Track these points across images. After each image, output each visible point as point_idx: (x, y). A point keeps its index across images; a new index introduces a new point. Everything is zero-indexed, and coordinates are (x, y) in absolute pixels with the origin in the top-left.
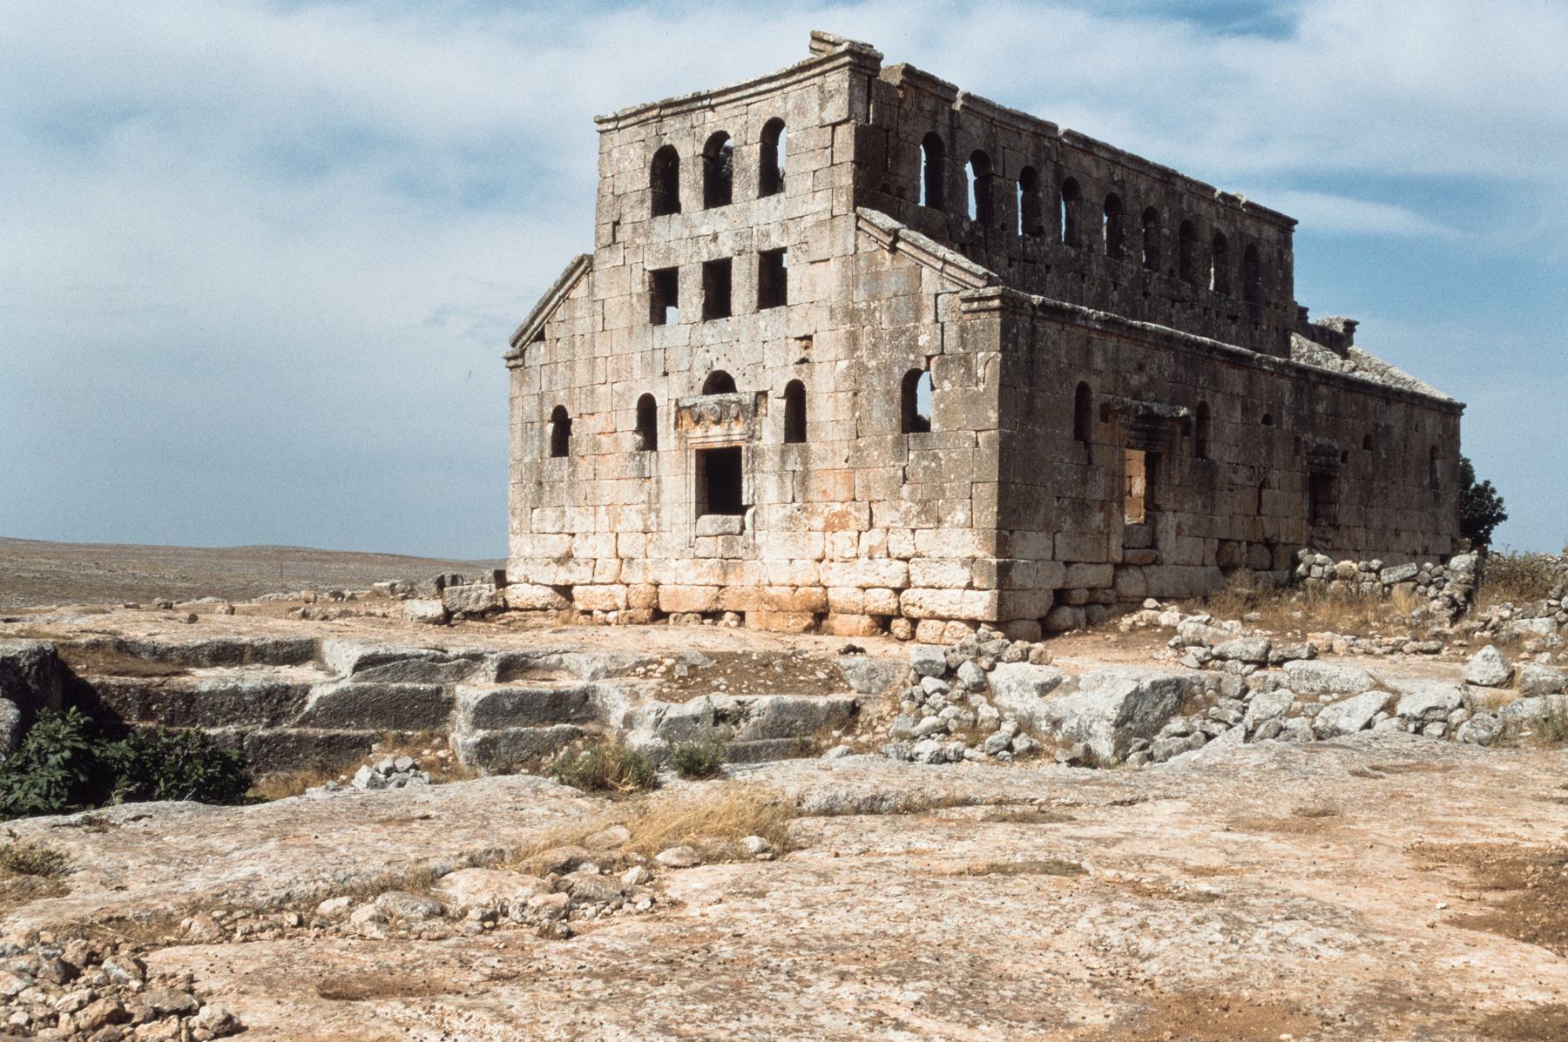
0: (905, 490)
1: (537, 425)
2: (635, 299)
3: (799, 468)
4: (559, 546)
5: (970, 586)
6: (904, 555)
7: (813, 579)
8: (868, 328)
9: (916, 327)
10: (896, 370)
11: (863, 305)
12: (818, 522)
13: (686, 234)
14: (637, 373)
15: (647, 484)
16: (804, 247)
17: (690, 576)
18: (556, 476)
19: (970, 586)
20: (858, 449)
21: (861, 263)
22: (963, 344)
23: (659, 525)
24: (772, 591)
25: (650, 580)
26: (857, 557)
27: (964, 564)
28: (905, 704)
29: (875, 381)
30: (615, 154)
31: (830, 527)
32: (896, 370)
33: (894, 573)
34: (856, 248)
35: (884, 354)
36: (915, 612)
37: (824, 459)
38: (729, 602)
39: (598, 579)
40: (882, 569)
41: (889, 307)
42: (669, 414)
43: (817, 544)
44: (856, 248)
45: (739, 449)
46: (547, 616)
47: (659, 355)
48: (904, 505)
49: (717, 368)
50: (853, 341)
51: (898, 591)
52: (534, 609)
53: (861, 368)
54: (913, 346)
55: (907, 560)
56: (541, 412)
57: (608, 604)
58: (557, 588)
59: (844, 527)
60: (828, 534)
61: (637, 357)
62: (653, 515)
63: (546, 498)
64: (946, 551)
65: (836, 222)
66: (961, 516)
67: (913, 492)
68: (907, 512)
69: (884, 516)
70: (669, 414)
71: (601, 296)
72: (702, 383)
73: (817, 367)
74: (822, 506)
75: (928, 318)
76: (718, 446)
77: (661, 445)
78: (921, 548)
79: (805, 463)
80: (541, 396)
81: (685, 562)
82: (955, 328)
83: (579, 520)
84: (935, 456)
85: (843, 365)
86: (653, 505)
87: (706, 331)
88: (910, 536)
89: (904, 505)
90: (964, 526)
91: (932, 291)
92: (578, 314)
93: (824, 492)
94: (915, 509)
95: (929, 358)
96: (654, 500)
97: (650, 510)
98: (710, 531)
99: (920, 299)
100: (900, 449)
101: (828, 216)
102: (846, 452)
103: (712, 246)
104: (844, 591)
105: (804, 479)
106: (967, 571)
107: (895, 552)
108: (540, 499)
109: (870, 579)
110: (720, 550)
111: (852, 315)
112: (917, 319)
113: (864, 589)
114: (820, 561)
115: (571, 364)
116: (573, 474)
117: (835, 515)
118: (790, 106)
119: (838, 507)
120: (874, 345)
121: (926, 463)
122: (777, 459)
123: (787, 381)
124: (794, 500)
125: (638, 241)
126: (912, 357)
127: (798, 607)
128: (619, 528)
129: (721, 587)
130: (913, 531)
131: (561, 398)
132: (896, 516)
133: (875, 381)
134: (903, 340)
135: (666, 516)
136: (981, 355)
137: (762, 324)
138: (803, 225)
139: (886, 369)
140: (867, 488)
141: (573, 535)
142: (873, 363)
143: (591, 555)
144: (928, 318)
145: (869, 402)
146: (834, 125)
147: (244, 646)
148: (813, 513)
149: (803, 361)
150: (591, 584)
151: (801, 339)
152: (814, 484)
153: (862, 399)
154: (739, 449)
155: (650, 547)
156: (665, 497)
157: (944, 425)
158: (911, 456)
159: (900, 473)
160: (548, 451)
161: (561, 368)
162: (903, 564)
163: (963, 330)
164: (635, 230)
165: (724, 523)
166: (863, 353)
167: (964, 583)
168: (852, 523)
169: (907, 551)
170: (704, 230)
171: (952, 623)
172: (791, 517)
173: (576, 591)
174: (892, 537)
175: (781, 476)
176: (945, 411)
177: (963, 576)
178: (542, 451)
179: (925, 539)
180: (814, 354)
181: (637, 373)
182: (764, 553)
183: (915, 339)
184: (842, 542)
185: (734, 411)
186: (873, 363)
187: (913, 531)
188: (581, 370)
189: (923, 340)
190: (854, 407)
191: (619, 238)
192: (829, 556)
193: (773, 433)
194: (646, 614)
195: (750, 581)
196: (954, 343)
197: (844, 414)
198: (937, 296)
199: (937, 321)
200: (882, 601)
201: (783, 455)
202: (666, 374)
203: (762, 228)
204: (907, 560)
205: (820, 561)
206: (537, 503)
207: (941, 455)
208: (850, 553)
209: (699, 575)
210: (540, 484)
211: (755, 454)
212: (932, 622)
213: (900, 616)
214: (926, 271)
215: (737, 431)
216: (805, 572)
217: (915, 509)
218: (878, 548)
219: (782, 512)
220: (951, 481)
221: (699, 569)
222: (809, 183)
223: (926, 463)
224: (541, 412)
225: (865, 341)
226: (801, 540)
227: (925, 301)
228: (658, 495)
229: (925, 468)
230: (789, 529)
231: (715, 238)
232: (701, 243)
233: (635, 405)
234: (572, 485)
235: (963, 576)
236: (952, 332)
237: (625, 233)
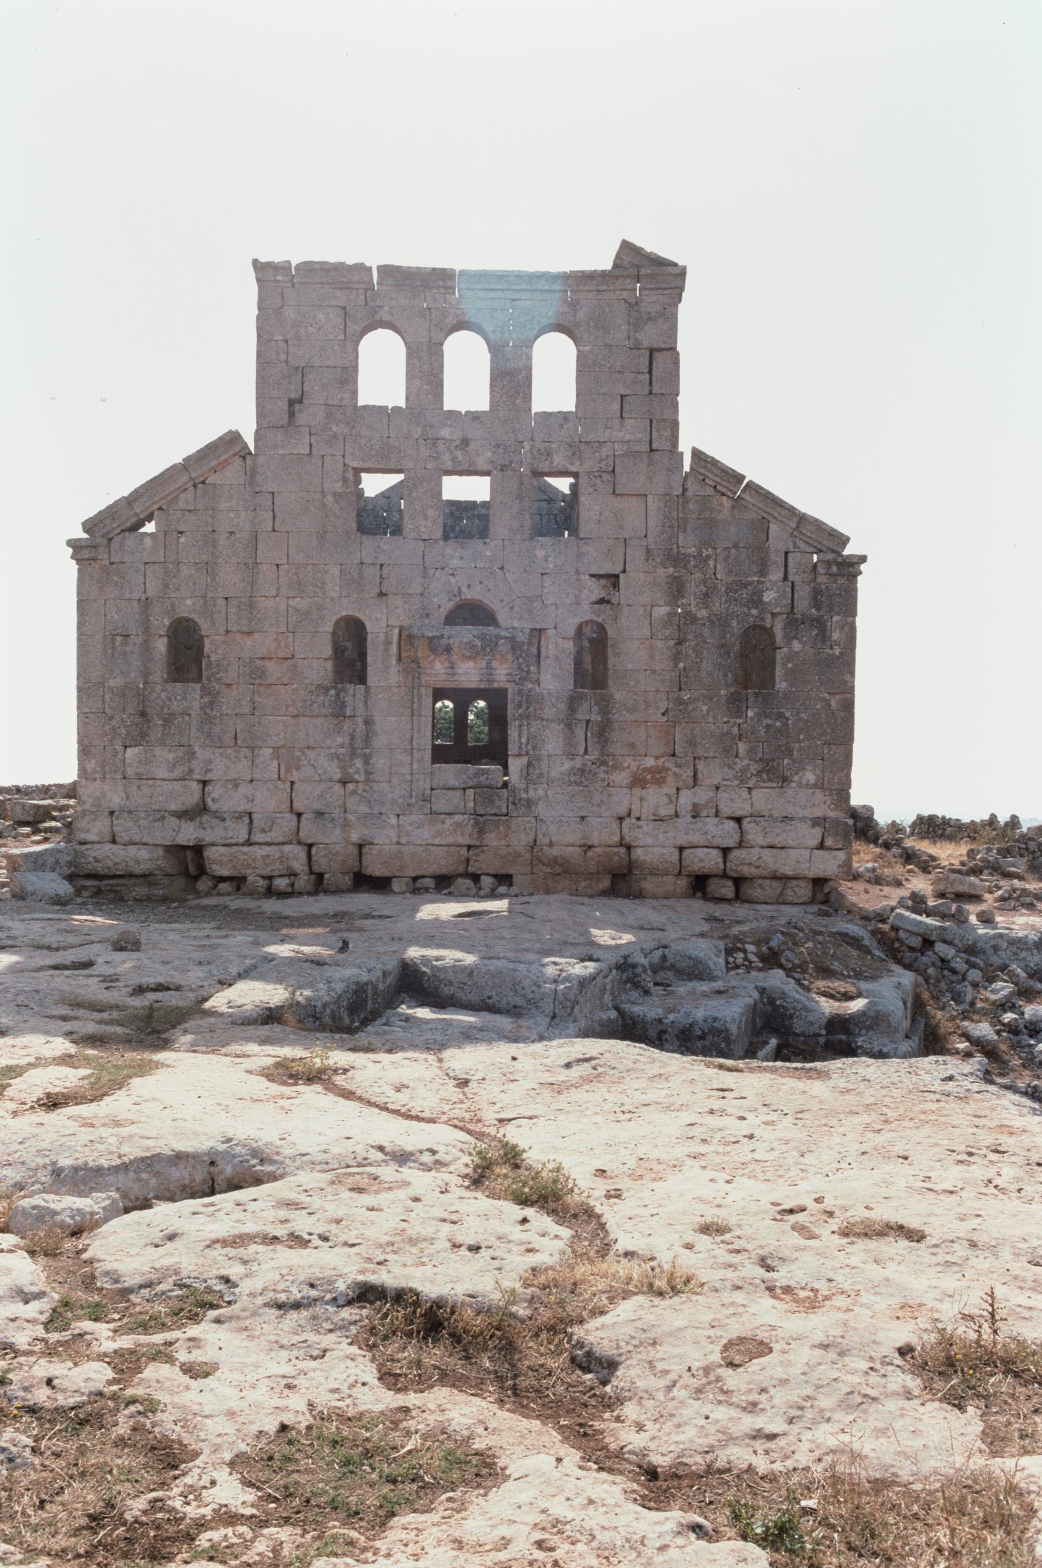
0: (742, 747)
1: (137, 640)
2: (330, 499)
3: (596, 717)
4: (191, 795)
5: (821, 846)
6: (738, 814)
7: (616, 839)
8: (698, 576)
9: (759, 582)
10: (735, 623)
11: (692, 550)
12: (621, 777)
13: (417, 432)
14: (333, 591)
15: (347, 725)
16: (606, 476)
17: (425, 834)
18: (175, 706)
19: (821, 846)
20: (680, 702)
21: (691, 506)
22: (817, 604)
23: (368, 773)
24: (555, 852)
25: (355, 837)
26: (677, 816)
27: (816, 822)
28: (931, 971)
29: (706, 632)
30: (289, 313)
31: (638, 781)
32: (735, 623)
33: (725, 833)
34: (685, 490)
35: (718, 606)
36: (746, 871)
37: (633, 710)
38: (484, 863)
39: (258, 837)
40: (712, 829)
41: (727, 557)
42: (388, 643)
43: (622, 800)
44: (685, 490)
45: (506, 690)
46: (150, 884)
47: (371, 572)
48: (740, 764)
49: (468, 595)
50: (677, 589)
51: (726, 851)
52: (131, 875)
53: (690, 618)
54: (756, 600)
55: (738, 820)
56: (146, 627)
57: (277, 868)
58: (176, 850)
59: (660, 782)
60: (637, 791)
61: (335, 570)
62: (359, 763)
63: (157, 734)
64: (790, 810)
65: (657, 456)
66: (810, 777)
67: (751, 751)
68: (744, 770)
69: (712, 773)
70: (388, 643)
71: (270, 487)
72: (443, 612)
73: (626, 610)
74: (629, 761)
75: (775, 575)
76: (472, 686)
77: (372, 678)
78: (761, 806)
79: (605, 711)
80: (146, 604)
81: (414, 818)
82: (808, 589)
83: (221, 766)
84: (780, 716)
85: (661, 611)
86: (361, 747)
87: (449, 551)
88: (745, 794)
89: (740, 764)
90: (815, 786)
91: (782, 547)
92: (223, 505)
93: (632, 746)
94: (754, 767)
95: (774, 615)
96: (359, 743)
97: (353, 754)
98: (453, 782)
99: (767, 554)
100: (736, 704)
101: (645, 448)
102: (664, 705)
103: (459, 454)
104: (657, 851)
105: (603, 732)
106: (818, 831)
107: (726, 810)
108: (143, 735)
109: (696, 838)
110: (471, 805)
111: (676, 559)
112: (763, 573)
113: (681, 849)
114: (621, 819)
115: (209, 568)
116: (211, 705)
117: (645, 770)
118: (581, 315)
119: (650, 762)
120: (706, 595)
121: (769, 722)
122: (563, 706)
123: (577, 620)
124: (586, 752)
125: (335, 428)
126: (754, 612)
127: (593, 869)
128: (295, 776)
129: (469, 847)
130: (750, 789)
131: (188, 607)
132: (730, 773)
133: (706, 632)
134: (744, 594)
135: (380, 763)
136: (836, 619)
137: (540, 553)
138: (605, 451)
139: (721, 622)
140: (692, 743)
141: (205, 783)
142: (704, 613)
143: (243, 806)
144: (775, 575)
145: (698, 653)
146: (652, 351)
147: (367, 984)
148: (615, 767)
149: (601, 601)
150: (248, 843)
151: (592, 576)
152: (616, 735)
153: (687, 649)
154: (505, 691)
155: (352, 802)
156: (380, 741)
157: (792, 685)
158: (750, 714)
159: (735, 730)
160: (158, 673)
161: (185, 571)
162: (732, 824)
163: (816, 592)
164: (329, 414)
165: (477, 774)
166: (691, 602)
167: (815, 842)
168: (670, 779)
169: (741, 808)
170: (445, 433)
171: (794, 883)
172: (582, 771)
173: (210, 853)
174: (723, 796)
175: (569, 726)
176: (793, 671)
177: (813, 836)
178: (146, 674)
179: (764, 798)
180: (624, 595)
181: (333, 591)
182: (541, 809)
183: (760, 593)
184: (655, 799)
185: (503, 646)
186: (704, 613)
187: (750, 789)
188: (230, 578)
189: (768, 597)
190: (676, 657)
191: (301, 418)
192: (635, 813)
193: (556, 677)
194: (348, 880)
195: (520, 841)
196: (806, 603)
197: (662, 663)
198: (786, 553)
199: (785, 578)
200: (708, 860)
201: (573, 703)
202: (382, 594)
203: (539, 445)
204: (738, 820)
205: (621, 819)
206: (140, 736)
207: (788, 714)
208: (665, 811)
209: (439, 833)
210: (143, 714)
211: (529, 699)
212: (768, 882)
213: (725, 875)
214: (773, 528)
215: (502, 674)
216: (603, 833)
217: (754, 767)
218: (705, 806)
219: (568, 765)
220: (799, 741)
221: (439, 826)
222: (616, 406)
223: (769, 722)
224: (146, 627)
225: (693, 586)
226: (597, 798)
227: (773, 556)
228: (367, 739)
229: (768, 726)
230: (579, 784)
231: (465, 442)
232: (441, 447)
233: (329, 628)
234: (207, 720)
235: (813, 836)
236: (803, 593)
237: (311, 415)
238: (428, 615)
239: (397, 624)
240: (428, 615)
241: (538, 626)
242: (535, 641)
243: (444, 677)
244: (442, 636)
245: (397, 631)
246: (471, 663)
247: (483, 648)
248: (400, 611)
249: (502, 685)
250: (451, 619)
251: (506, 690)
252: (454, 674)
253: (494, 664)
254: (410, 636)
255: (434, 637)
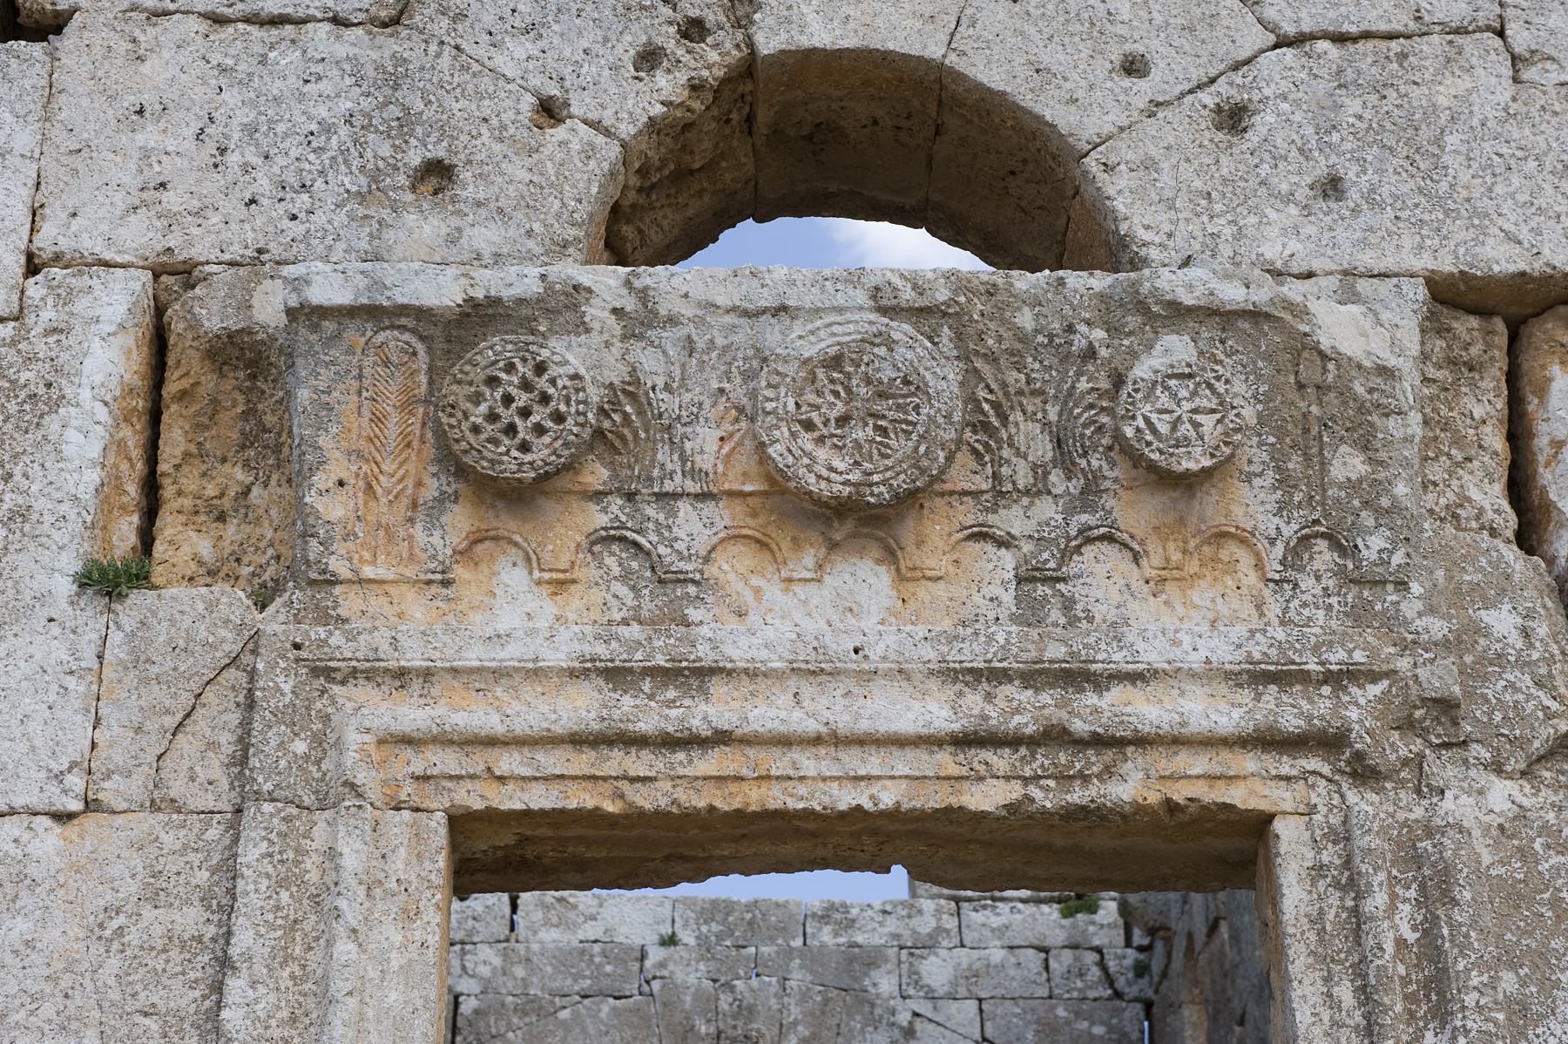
238: (437, 174)
239: (139, 236)
240: (437, 174)
241: (1500, 258)
242: (1484, 405)
243: (582, 706)
244: (564, 306)
245: (117, 301)
246: (864, 581)
247: (985, 427)
248: (172, 140)
249: (1192, 780)
250: (673, 197)
251: (1260, 825)
252: (694, 676)
253: (1102, 579)
254: (247, 358)
255: (480, 316)
